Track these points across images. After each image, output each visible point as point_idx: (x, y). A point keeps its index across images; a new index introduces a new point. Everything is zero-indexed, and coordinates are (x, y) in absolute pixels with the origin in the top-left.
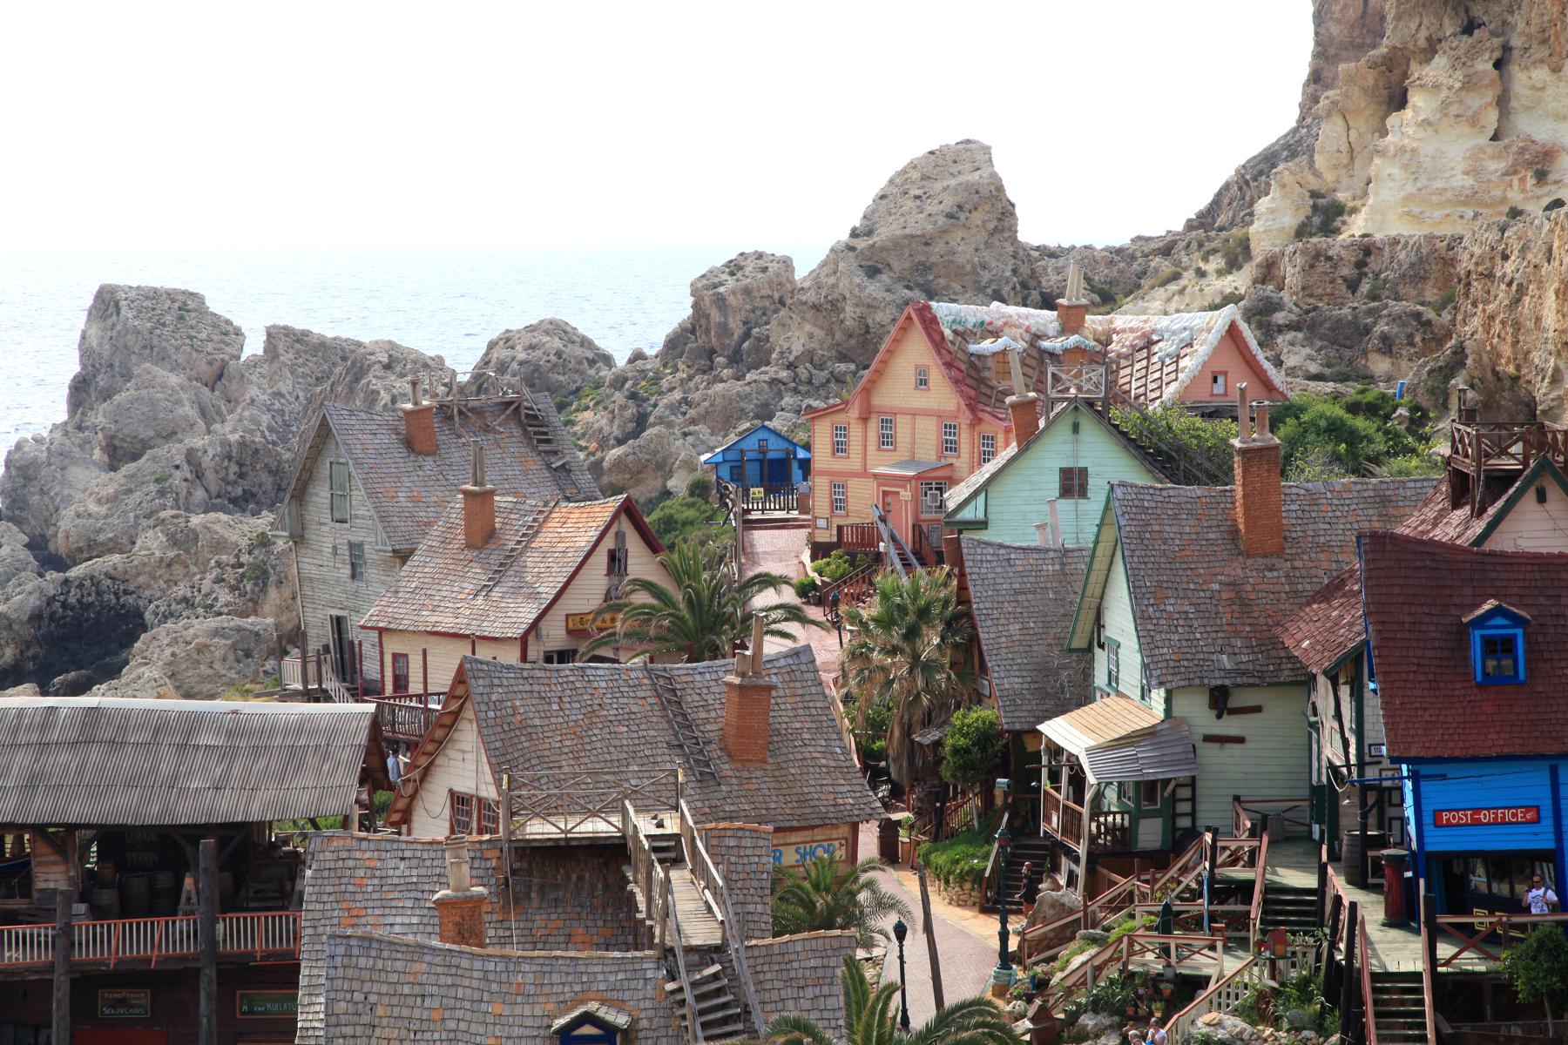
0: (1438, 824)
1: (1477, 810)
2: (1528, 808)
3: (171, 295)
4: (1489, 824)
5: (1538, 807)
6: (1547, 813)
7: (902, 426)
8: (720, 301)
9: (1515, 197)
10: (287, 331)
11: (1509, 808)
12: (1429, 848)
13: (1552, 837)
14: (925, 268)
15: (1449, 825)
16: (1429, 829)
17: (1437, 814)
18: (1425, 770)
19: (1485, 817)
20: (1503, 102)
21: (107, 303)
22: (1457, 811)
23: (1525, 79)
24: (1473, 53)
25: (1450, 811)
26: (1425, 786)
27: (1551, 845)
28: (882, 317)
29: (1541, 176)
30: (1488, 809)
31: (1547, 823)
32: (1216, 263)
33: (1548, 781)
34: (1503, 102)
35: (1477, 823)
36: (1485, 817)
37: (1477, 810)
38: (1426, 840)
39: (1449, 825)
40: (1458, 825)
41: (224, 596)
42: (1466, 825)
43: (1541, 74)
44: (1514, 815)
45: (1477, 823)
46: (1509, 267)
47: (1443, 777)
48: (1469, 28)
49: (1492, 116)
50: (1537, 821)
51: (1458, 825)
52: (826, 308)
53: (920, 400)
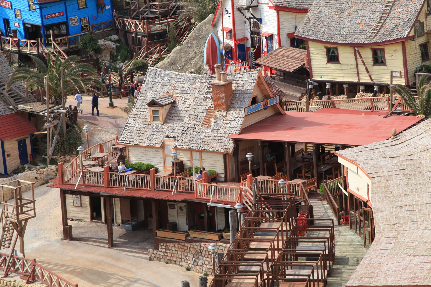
0: (45, 18)
1: (52, 14)
2: (61, 12)
4: (55, 17)
5: (63, 12)
6: (65, 13)
11: (58, 13)
12: (44, 24)
13: (66, 18)
15: (48, 18)
16: (44, 20)
17: (45, 16)
18: (42, 6)
19: (54, 15)
22: (49, 15)
25: (47, 15)
26: (43, 10)
27: (65, 20)
30: (54, 14)
31: (65, 15)
33: (64, 6)
35: (53, 17)
36: (54, 15)
37: (52, 14)
38: (44, 22)
39: (48, 18)
40: (49, 18)
42: (51, 18)
44: (59, 14)
45: (53, 17)
47: (46, 7)
50: (63, 15)
51: (49, 18)
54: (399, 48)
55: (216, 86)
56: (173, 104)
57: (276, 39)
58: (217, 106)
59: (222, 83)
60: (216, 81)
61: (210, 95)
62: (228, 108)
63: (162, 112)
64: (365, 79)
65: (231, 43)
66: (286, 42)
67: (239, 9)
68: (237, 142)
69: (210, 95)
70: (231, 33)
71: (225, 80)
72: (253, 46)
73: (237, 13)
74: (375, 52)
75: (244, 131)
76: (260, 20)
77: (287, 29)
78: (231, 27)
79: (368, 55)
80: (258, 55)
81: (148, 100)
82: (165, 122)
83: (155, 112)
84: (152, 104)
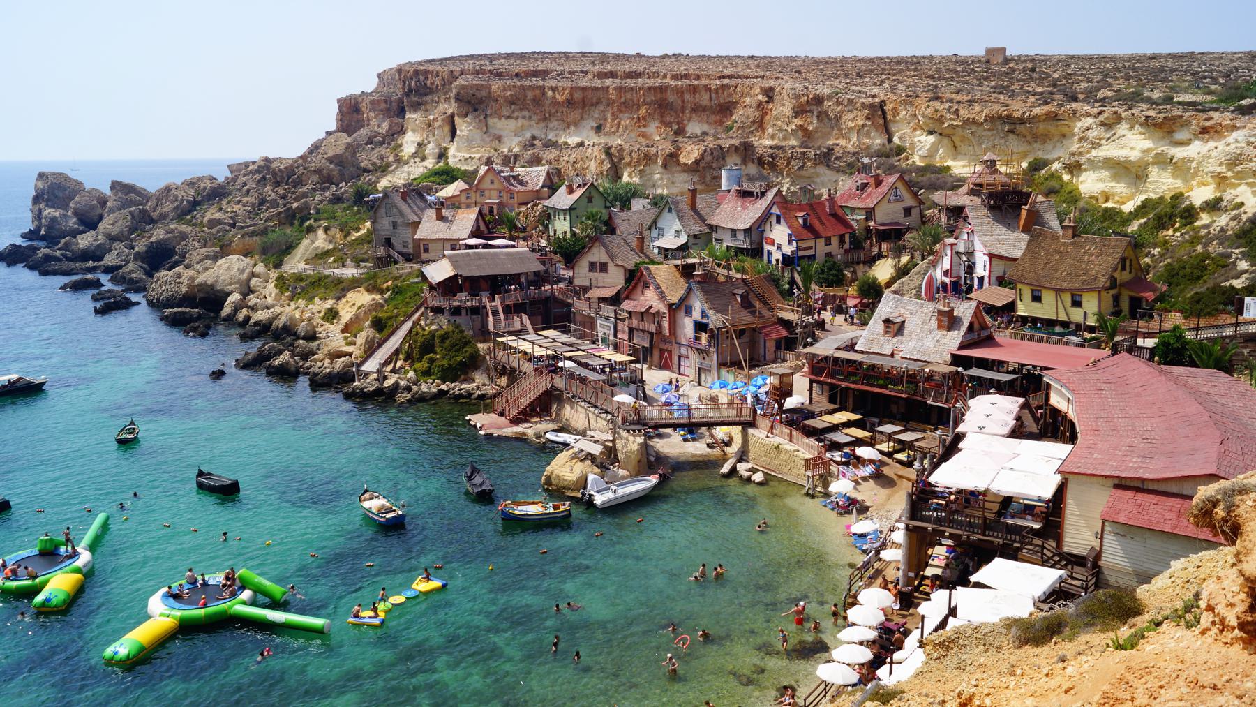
3: (60, 174)
7: (487, 193)
8: (280, 170)
9: (493, 145)
10: (117, 182)
14: (341, 162)
20: (486, 125)
21: (41, 176)
23: (491, 121)
24: (479, 115)
28: (335, 173)
29: (499, 141)
32: (417, 160)
34: (486, 125)
41: (197, 244)
43: (496, 120)
46: (566, 158)
48: (476, 110)
49: (485, 129)
52: (318, 171)
53: (491, 187)
54: (1096, 295)
55: (940, 312)
56: (903, 322)
57: (986, 280)
58: (940, 327)
59: (946, 309)
60: (942, 308)
61: (934, 318)
62: (949, 329)
63: (894, 328)
64: (1063, 317)
65: (947, 280)
66: (993, 279)
67: (957, 253)
68: (953, 356)
69: (934, 318)
70: (946, 273)
71: (949, 307)
72: (966, 283)
73: (955, 257)
74: (1073, 296)
75: (960, 348)
76: (974, 264)
77: (999, 271)
78: (948, 267)
79: (1068, 299)
80: (970, 290)
81: (884, 317)
82: (895, 335)
83: (887, 327)
84: (887, 321)
